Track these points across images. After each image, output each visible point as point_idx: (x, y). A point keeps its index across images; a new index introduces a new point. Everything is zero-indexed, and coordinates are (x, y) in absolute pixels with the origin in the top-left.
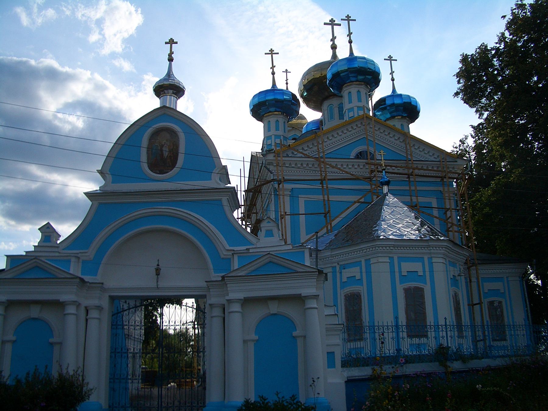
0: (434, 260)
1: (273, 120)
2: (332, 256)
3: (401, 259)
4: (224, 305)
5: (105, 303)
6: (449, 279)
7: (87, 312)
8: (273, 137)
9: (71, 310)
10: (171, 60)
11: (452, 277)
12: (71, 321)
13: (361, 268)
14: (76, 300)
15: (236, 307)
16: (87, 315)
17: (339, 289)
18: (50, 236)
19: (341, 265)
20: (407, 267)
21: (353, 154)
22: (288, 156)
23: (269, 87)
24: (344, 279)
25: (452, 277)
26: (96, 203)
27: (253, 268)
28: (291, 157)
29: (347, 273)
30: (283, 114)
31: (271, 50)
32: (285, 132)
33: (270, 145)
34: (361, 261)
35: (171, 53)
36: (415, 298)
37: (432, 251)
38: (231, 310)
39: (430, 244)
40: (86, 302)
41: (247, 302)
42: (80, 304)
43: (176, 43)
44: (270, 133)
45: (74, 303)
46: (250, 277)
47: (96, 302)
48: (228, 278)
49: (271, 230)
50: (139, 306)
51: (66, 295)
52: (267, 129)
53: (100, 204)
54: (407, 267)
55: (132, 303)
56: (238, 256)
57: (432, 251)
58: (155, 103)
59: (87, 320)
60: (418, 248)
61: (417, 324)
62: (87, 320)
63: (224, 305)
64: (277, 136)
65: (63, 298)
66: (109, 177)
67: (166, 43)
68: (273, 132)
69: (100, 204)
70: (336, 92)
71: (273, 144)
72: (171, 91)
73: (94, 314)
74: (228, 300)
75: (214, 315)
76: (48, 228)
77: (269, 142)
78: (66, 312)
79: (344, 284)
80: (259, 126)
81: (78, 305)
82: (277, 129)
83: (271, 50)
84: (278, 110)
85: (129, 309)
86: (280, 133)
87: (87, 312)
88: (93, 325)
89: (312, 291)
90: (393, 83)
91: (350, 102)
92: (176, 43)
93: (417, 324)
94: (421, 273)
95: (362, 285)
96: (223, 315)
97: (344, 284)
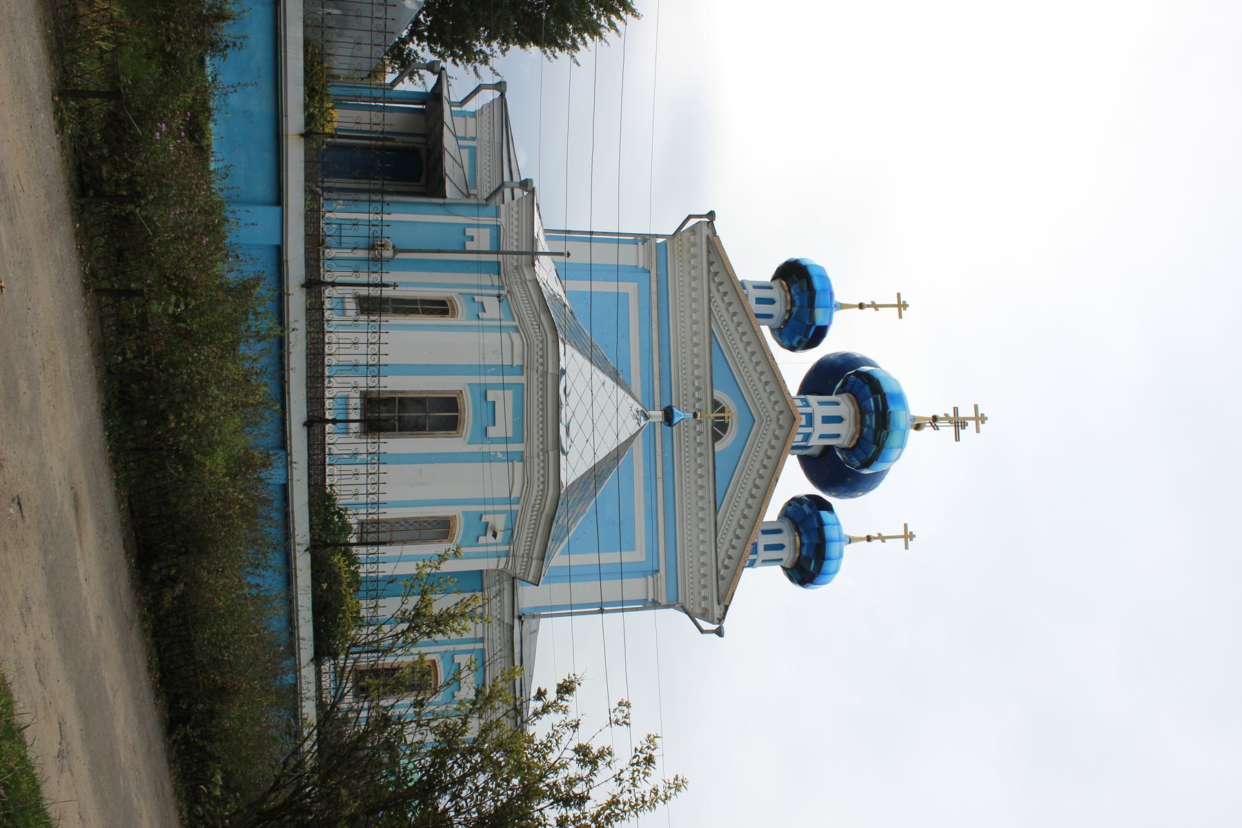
0: (518, 466)
3: (521, 393)
6: (481, 508)
11: (485, 519)
20: (504, 402)
21: (719, 395)
22: (710, 264)
25: (485, 519)
28: (709, 271)
29: (492, 305)
30: (789, 312)
31: (905, 306)
36: (439, 414)
37: (536, 459)
39: (551, 453)
44: (750, 288)
54: (504, 402)
57: (536, 459)
60: (543, 475)
61: (386, 415)
68: (754, 294)
80: (766, 275)
82: (760, 301)
83: (905, 306)
90: (861, 539)
91: (820, 403)
93: (386, 415)
94: (492, 432)
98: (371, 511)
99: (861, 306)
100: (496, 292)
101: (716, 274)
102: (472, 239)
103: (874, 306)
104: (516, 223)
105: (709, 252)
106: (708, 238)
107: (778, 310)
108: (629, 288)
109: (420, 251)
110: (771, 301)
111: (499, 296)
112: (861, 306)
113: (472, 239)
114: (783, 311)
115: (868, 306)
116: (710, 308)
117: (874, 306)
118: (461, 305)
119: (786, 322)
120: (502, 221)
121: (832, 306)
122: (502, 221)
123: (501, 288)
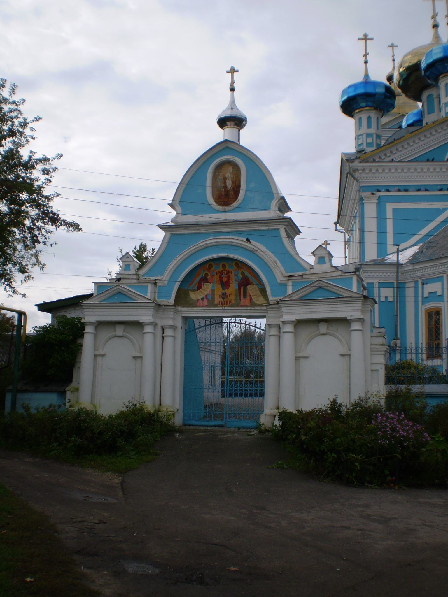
1: (364, 116)
2: (414, 270)
4: (279, 325)
5: (179, 323)
7: (163, 330)
8: (365, 135)
9: (148, 329)
10: (232, 90)
12: (148, 339)
13: (443, 285)
14: (152, 321)
15: (289, 328)
16: (163, 333)
17: (420, 304)
18: (129, 265)
19: (423, 280)
22: (374, 161)
23: (359, 78)
24: (426, 295)
26: (168, 234)
27: (304, 293)
28: (378, 162)
29: (429, 288)
30: (376, 108)
32: (378, 129)
33: (362, 144)
34: (443, 276)
35: (233, 82)
38: (284, 330)
40: (160, 323)
41: (299, 323)
42: (156, 324)
43: (237, 71)
44: (361, 132)
45: (151, 323)
46: (304, 300)
47: (170, 322)
48: (283, 302)
49: (323, 258)
50: (208, 325)
51: (145, 316)
52: (359, 125)
53: (172, 235)
55: (203, 323)
56: (293, 282)
58: (219, 135)
59: (163, 337)
62: (163, 337)
63: (279, 325)
64: (369, 135)
65: (142, 319)
66: (179, 208)
67: (228, 72)
68: (364, 129)
69: (172, 235)
70: (434, 83)
71: (365, 144)
72: (233, 123)
73: (169, 332)
74: (283, 322)
75: (271, 334)
76: (128, 257)
77: (360, 142)
78: (145, 331)
79: (425, 300)
80: (350, 122)
81: (154, 324)
82: (369, 126)
84: (370, 104)
85: (200, 327)
86: (373, 130)
87: (163, 330)
88: (168, 341)
89: (357, 315)
92: (237, 71)
95: (444, 302)
96: (278, 334)
97: (425, 300)
98: (420, 351)
99: (366, 62)
100: (420, 286)
101: (380, 157)
102: (386, 298)
103: (366, 55)
104: (377, 274)
105: (368, 162)
106: (360, 162)
107: (374, 115)
108: (390, 208)
109: (396, 326)
110: (369, 118)
111: (423, 284)
112: (366, 62)
113: (386, 298)
114: (374, 111)
115: (366, 58)
116: (399, 162)
117: (366, 55)
118: (433, 304)
119: (381, 110)
120: (376, 281)
121: (367, 82)
122: (376, 281)
123: (416, 282)
